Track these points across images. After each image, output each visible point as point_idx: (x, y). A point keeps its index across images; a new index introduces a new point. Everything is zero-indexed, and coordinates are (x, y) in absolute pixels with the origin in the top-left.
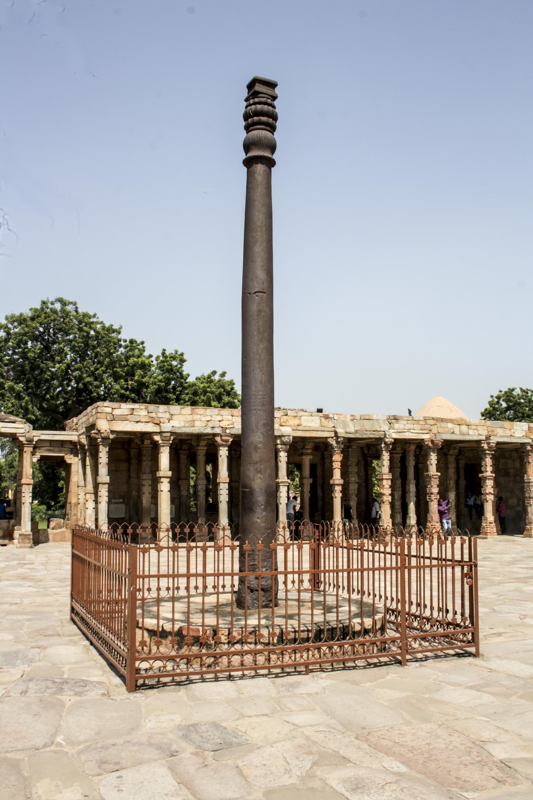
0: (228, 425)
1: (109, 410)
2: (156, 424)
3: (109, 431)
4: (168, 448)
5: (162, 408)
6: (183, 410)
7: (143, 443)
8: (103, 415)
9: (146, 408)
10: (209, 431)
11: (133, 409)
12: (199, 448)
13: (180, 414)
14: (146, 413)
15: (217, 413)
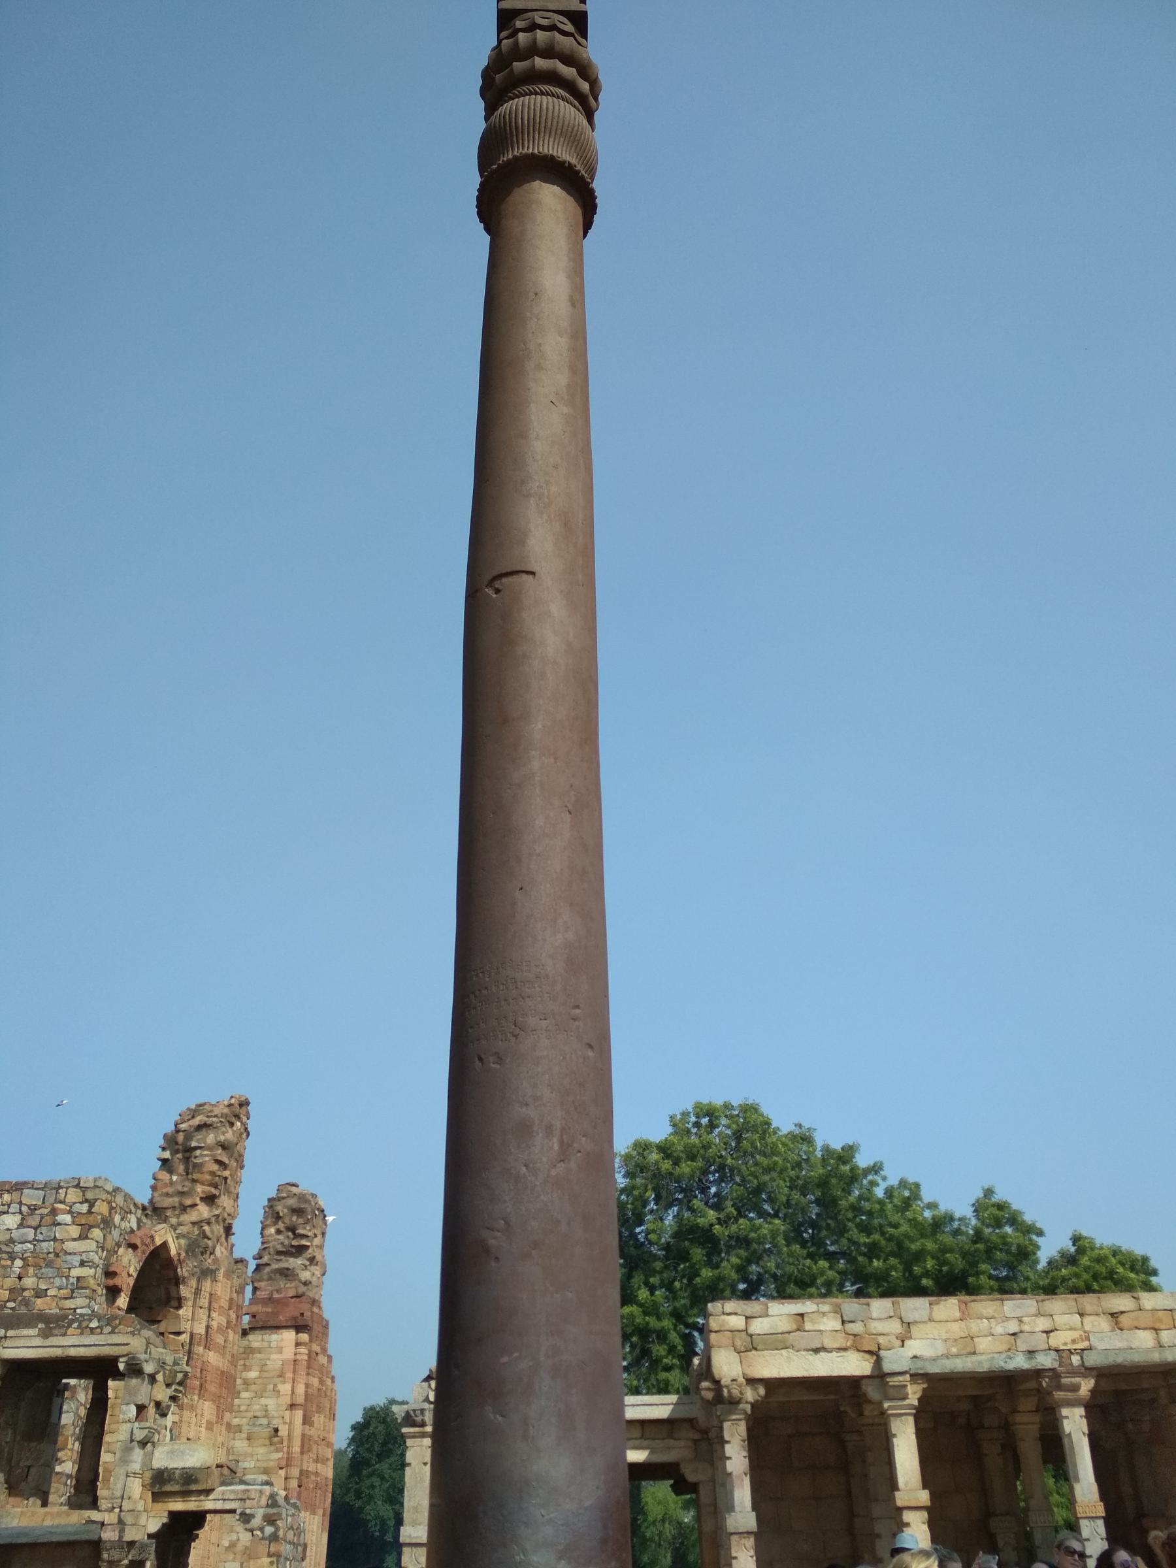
0: (1074, 1341)
1: (737, 1322)
2: (870, 1352)
3: (741, 1380)
4: (911, 1419)
5: (880, 1306)
6: (935, 1308)
7: (861, 1414)
8: (723, 1338)
9: (837, 1310)
10: (1020, 1362)
11: (802, 1315)
12: (1020, 1418)
13: (931, 1320)
14: (837, 1325)
15: (1033, 1310)
